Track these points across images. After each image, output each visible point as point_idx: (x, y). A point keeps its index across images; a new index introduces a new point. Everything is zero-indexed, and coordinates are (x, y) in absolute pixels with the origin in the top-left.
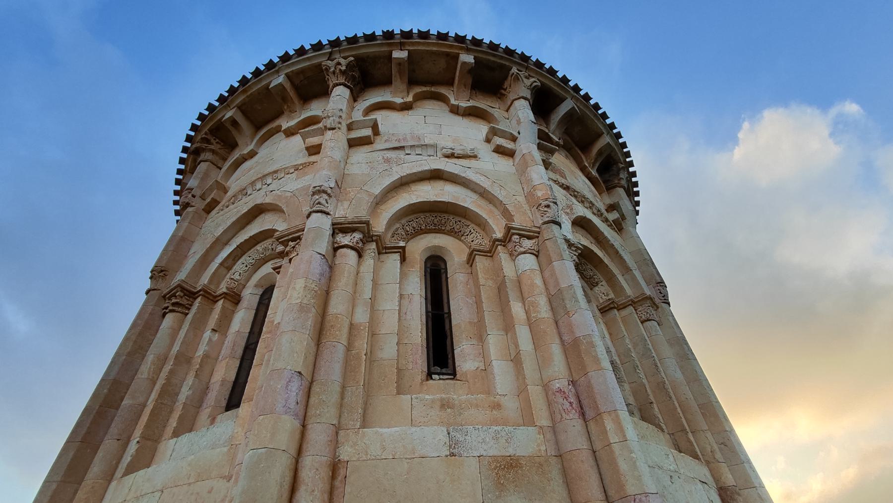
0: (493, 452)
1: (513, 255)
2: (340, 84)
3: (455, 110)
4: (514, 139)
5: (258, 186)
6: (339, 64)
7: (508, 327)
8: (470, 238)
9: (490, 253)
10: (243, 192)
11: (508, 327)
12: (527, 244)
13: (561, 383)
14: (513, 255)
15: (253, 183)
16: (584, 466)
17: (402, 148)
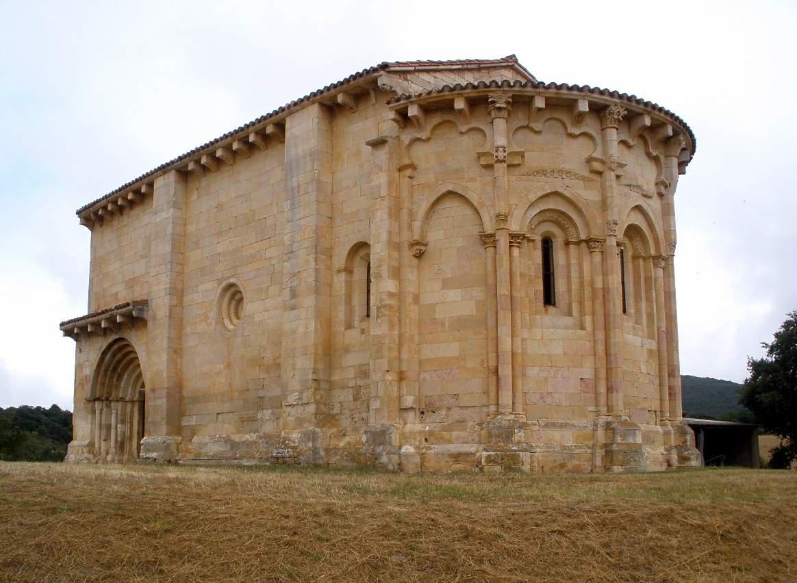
0: (649, 347)
1: (656, 266)
2: (614, 128)
3: (648, 154)
4: (666, 187)
5: (556, 175)
6: (619, 112)
7: (648, 299)
8: (635, 244)
9: (645, 259)
10: (542, 172)
11: (648, 299)
12: (663, 264)
13: (664, 329)
14: (656, 266)
15: (553, 171)
16: (665, 354)
17: (630, 186)
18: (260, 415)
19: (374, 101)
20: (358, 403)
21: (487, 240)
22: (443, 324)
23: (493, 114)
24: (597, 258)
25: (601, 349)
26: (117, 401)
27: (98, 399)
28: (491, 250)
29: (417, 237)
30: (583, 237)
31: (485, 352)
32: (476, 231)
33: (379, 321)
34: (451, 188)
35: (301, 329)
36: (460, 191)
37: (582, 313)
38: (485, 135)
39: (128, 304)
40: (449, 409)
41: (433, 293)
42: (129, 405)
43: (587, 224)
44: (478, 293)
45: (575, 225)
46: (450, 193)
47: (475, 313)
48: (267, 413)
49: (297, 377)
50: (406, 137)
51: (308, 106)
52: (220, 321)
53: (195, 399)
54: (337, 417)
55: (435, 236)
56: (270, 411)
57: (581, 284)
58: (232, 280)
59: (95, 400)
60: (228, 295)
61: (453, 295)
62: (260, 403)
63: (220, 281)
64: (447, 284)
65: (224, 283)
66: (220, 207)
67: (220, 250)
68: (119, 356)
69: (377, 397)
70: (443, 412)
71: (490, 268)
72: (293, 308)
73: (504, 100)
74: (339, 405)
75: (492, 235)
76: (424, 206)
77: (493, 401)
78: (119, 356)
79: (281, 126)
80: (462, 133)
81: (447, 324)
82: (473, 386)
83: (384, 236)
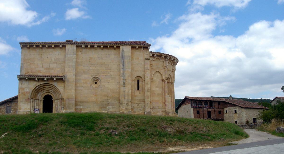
18: (108, 107)
19: (143, 49)
20: (139, 107)
21: (163, 80)
22: (156, 94)
23: (167, 60)
24: (172, 85)
25: (172, 101)
26: (37, 99)
27: (33, 99)
28: (164, 83)
29: (152, 78)
30: (171, 82)
31: (162, 99)
32: (161, 79)
33: (148, 92)
34: (158, 70)
35: (126, 91)
36: (159, 71)
37: (170, 95)
38: (164, 62)
39: (62, 76)
40: (157, 109)
41: (154, 88)
42: (40, 101)
43: (171, 80)
44: (161, 89)
45: (170, 80)
46: (158, 71)
47: (161, 93)
48: (110, 107)
49: (126, 100)
50: (151, 59)
51: (128, 46)
52: (91, 85)
53: (81, 102)
54: (133, 109)
55: (154, 78)
56: (111, 106)
57: (170, 90)
58: (96, 76)
59: (31, 99)
60: (93, 79)
61: (157, 89)
62: (108, 105)
63: (92, 76)
64: (156, 87)
65: (94, 77)
66: (91, 58)
67: (91, 68)
68: (41, 88)
69: (147, 106)
70: (156, 109)
71: (164, 85)
72: (124, 86)
73: (169, 58)
74: (133, 107)
75: (165, 80)
76: (154, 73)
77: (164, 108)
78: (41, 88)
79: (118, 47)
80: (160, 61)
81: (157, 94)
82: (161, 105)
83: (149, 77)
